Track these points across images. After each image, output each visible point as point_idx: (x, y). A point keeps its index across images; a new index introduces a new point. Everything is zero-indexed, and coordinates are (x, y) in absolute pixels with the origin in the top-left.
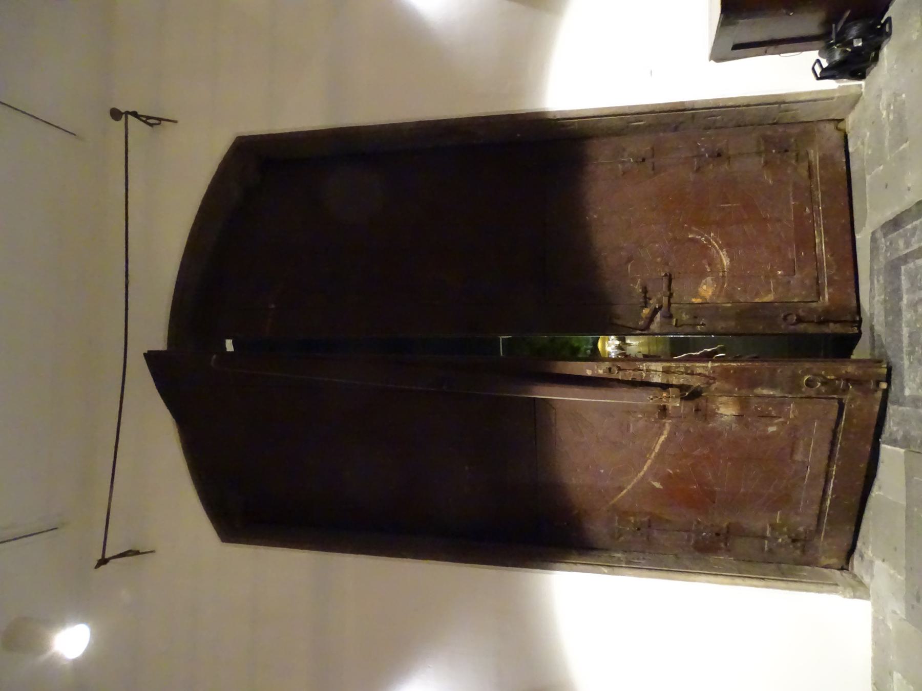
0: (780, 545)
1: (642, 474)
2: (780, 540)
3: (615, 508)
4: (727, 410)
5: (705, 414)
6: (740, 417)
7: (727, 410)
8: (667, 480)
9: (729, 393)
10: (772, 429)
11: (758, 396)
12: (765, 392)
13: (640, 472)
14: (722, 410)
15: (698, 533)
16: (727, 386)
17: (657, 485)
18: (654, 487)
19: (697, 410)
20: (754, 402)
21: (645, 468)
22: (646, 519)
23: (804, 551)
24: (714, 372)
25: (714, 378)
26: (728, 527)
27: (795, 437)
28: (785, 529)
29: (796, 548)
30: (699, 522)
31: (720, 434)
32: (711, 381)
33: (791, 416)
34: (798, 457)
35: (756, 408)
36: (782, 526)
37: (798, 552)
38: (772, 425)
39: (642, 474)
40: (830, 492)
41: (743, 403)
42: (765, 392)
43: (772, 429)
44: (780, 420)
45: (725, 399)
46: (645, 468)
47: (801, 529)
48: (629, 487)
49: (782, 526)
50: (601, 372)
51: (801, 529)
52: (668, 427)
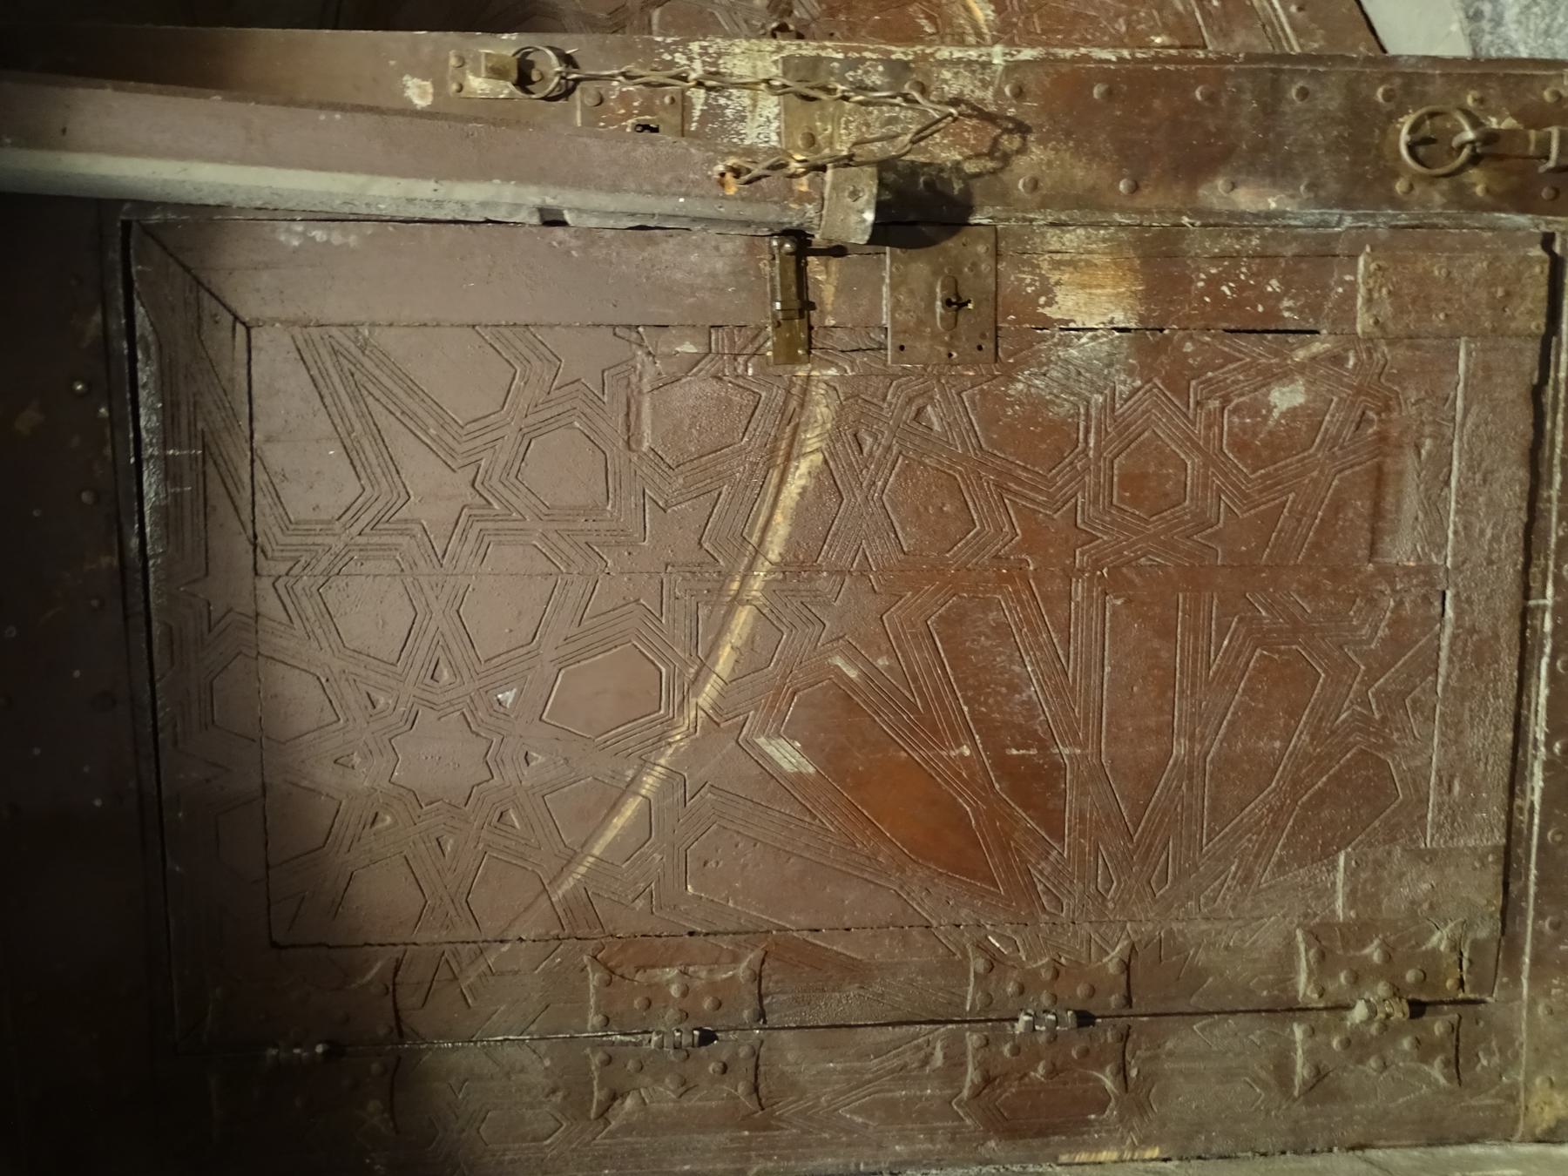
0: (1357, 1045)
1: (708, 693)
2: (1359, 1012)
3: (579, 923)
4: (1090, 304)
5: (990, 326)
6: (1147, 339)
7: (1090, 304)
8: (839, 723)
9: (1083, 205)
10: (1286, 397)
11: (1217, 222)
12: (1246, 199)
13: (697, 681)
14: (1068, 304)
15: (995, 1019)
16: (1082, 174)
17: (787, 756)
18: (770, 773)
19: (955, 303)
20: (1200, 244)
21: (725, 660)
22: (742, 970)
23: (1455, 1066)
24: (1019, 93)
25: (1022, 129)
26: (1126, 967)
27: (1382, 438)
28: (1374, 952)
29: (1425, 1050)
30: (994, 961)
31: (1062, 436)
32: (1010, 143)
33: (1363, 322)
34: (1402, 550)
35: (1215, 282)
36: (1358, 933)
37: (1436, 1071)
38: (1284, 375)
39: (708, 693)
40: (1539, 729)
41: (1159, 262)
42: (1246, 199)
43: (1286, 397)
44: (1317, 347)
45: (1072, 239)
46: (725, 660)
47: (1439, 940)
48: (649, 783)
49: (1358, 933)
50: (478, 84)
51: (1439, 940)
52: (822, 410)
